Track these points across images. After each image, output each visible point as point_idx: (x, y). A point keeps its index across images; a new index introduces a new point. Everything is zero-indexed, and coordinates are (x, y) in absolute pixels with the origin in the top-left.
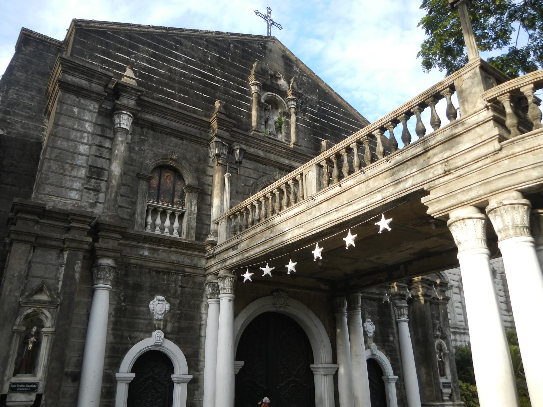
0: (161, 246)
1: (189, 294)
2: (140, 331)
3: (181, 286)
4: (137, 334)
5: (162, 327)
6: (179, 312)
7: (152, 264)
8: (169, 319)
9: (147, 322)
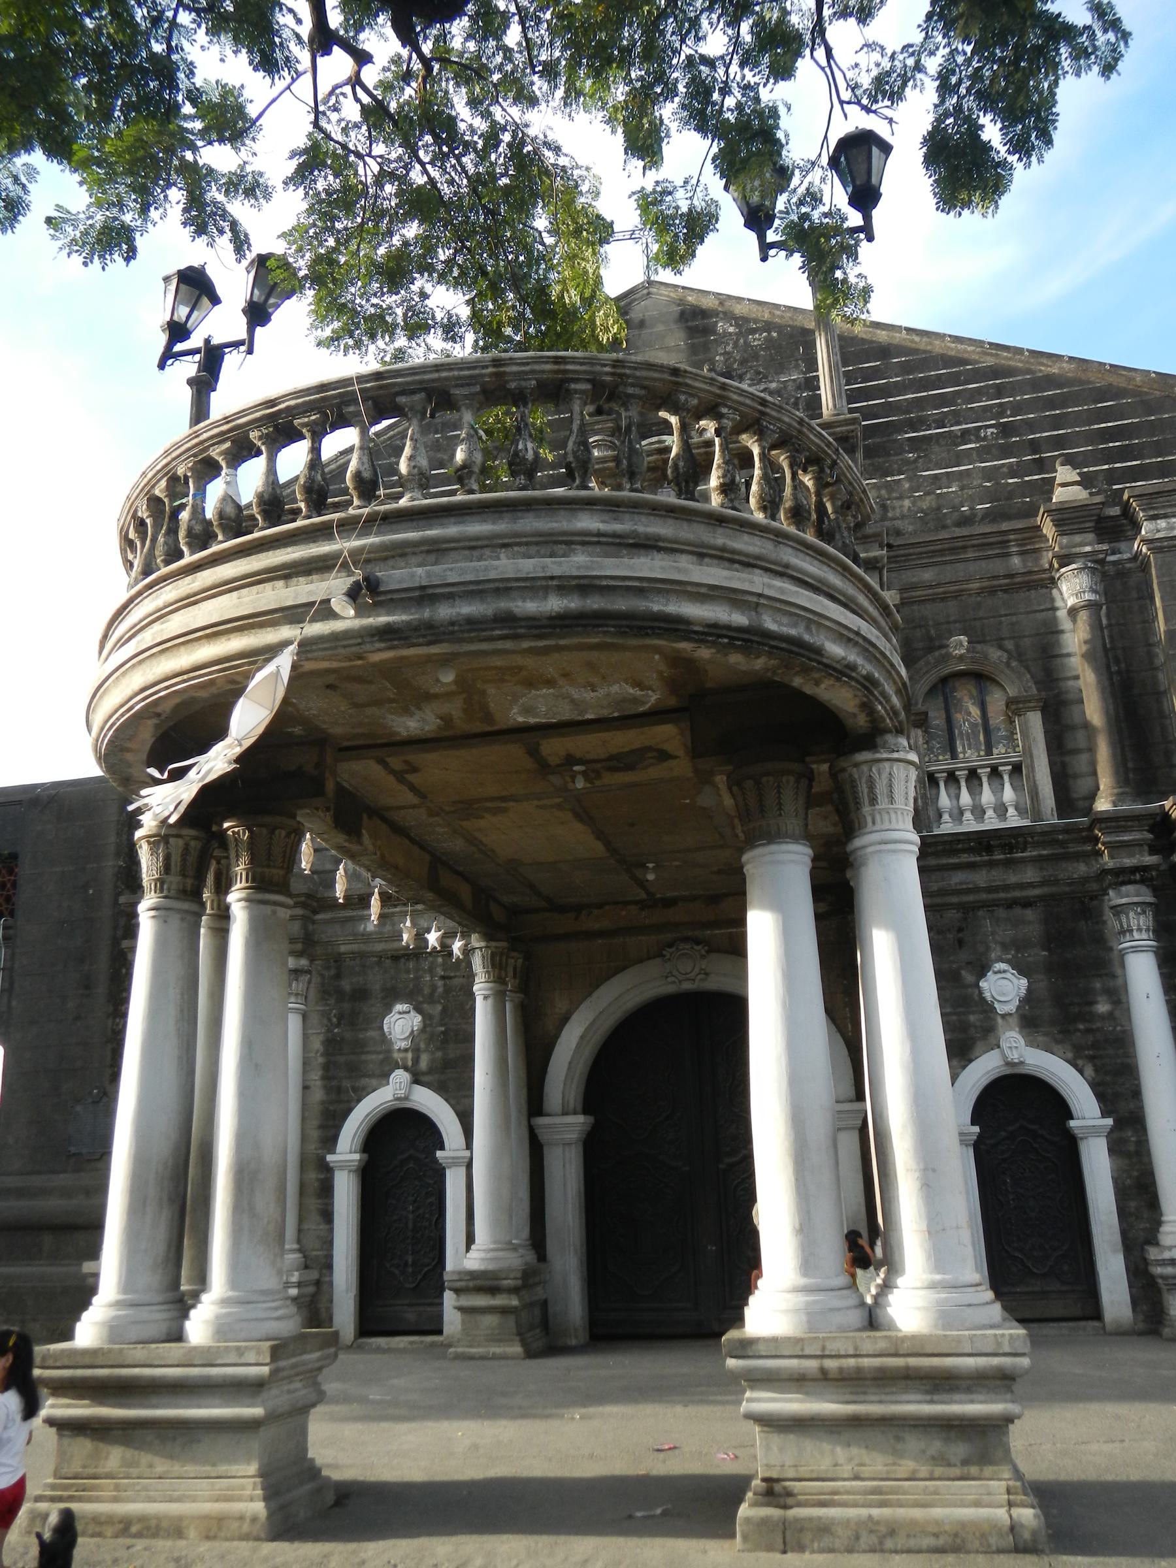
0: (395, 906)
1: (460, 990)
2: (369, 1076)
3: (443, 978)
4: (364, 1081)
5: (410, 1063)
6: (443, 1029)
7: (379, 947)
8: (422, 1046)
9: (381, 1056)
